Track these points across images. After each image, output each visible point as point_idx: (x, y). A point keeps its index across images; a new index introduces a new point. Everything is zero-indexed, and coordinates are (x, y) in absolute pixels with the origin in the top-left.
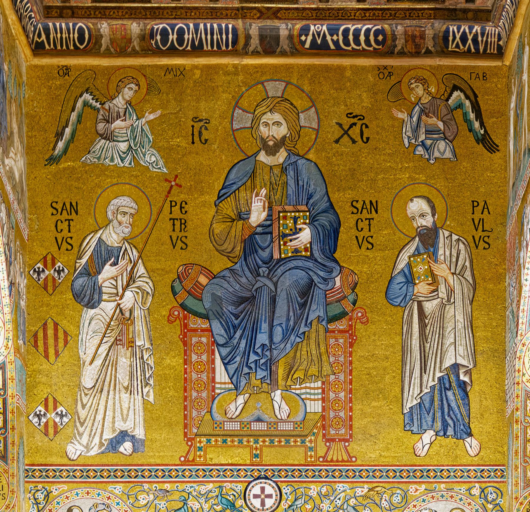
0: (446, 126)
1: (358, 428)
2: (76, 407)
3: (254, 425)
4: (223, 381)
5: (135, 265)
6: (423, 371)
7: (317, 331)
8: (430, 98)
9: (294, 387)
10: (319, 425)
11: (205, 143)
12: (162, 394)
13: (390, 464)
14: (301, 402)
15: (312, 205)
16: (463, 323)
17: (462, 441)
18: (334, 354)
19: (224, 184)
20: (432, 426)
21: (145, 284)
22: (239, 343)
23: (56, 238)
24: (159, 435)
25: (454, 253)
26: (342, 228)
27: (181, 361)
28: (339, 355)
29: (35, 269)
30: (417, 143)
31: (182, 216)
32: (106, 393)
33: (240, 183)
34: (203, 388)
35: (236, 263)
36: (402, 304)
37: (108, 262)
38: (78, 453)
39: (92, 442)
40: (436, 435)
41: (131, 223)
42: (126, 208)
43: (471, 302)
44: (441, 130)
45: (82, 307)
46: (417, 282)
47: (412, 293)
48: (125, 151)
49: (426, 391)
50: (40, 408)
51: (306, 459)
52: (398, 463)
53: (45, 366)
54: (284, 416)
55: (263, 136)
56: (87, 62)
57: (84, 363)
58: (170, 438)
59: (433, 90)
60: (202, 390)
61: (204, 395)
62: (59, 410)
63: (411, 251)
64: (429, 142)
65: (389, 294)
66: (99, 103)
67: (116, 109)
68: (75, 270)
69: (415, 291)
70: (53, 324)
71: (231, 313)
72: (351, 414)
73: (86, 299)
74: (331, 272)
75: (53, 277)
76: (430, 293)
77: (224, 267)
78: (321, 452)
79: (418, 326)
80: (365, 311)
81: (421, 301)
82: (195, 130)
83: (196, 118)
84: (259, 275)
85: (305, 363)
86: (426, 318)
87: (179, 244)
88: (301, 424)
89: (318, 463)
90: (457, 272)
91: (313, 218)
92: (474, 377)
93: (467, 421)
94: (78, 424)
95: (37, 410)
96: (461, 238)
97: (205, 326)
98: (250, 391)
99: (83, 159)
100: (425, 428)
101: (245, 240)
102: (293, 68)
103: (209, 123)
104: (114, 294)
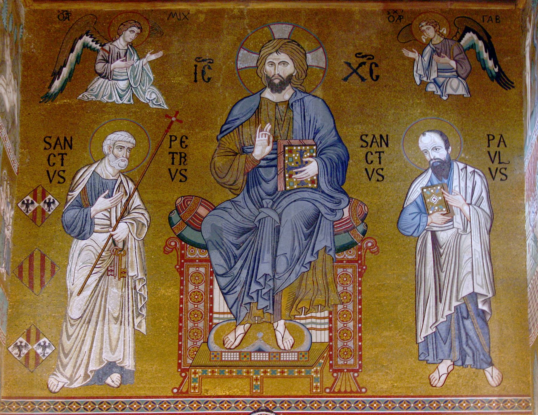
0: (458, 65)
1: (368, 358)
2: (61, 338)
3: (254, 355)
4: (222, 311)
5: (130, 197)
6: (438, 300)
7: (324, 260)
8: (442, 39)
9: (298, 317)
10: (325, 355)
11: (208, 82)
12: (155, 324)
13: (404, 395)
14: (306, 332)
15: (319, 139)
16: (480, 252)
17: (482, 370)
18: (342, 284)
19: (227, 120)
20: (449, 356)
21: (141, 216)
22: (239, 274)
23: (48, 171)
24: (150, 366)
25: (470, 184)
26: (351, 161)
27: (177, 291)
28: (347, 284)
29: (24, 201)
30: (429, 81)
31: (182, 150)
32: (95, 324)
33: (244, 119)
34: (200, 319)
35: (238, 195)
36: (415, 234)
37: (102, 194)
38: (61, 385)
39: (76, 374)
40: (454, 364)
41: (128, 156)
42: (123, 143)
43: (489, 232)
44: (453, 69)
45: (72, 238)
46: (431, 212)
47: (425, 224)
48: (124, 89)
49: (441, 320)
50: (21, 339)
51: (311, 390)
52: (412, 394)
53: (30, 296)
54: (288, 346)
55: (268, 75)
56: (89, 6)
57: (71, 294)
58: (162, 370)
59: (445, 32)
60: (198, 321)
61: (201, 325)
62: (41, 341)
63: (424, 183)
64: (441, 80)
65: (401, 224)
66: (99, 45)
67: (117, 50)
68: (67, 202)
69: (429, 221)
70: (39, 255)
71: (232, 244)
72: (360, 344)
73: (77, 231)
74: (340, 203)
75: (42, 209)
76: (445, 223)
77: (225, 199)
78: (328, 382)
79: (432, 255)
80: (376, 241)
81: (435, 231)
82: (197, 69)
83: (199, 58)
84: (262, 207)
85: (311, 292)
86: (441, 248)
87: (179, 177)
88: (306, 354)
89: (324, 394)
90: (473, 203)
91: (321, 151)
92: (493, 305)
93: (487, 350)
94: (62, 355)
95: (17, 341)
96: (476, 170)
97: (205, 256)
98: (251, 322)
99: (80, 96)
100: (442, 357)
101: (248, 172)
102: (300, 12)
103: (212, 63)
104: (107, 225)
